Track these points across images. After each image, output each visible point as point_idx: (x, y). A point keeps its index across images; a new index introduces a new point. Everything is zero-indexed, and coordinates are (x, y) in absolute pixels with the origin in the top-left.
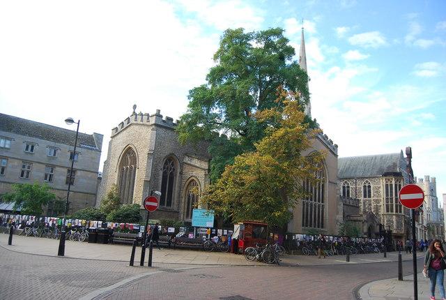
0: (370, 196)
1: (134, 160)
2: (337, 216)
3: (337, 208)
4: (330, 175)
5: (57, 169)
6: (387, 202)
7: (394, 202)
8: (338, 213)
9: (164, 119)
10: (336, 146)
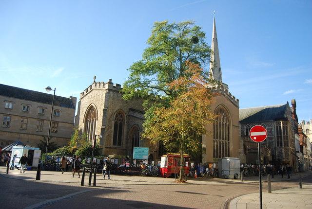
1: (95, 115)
3: (239, 144)
4: (234, 122)
5: (45, 122)
6: (278, 139)
9: (115, 85)
10: (238, 100)
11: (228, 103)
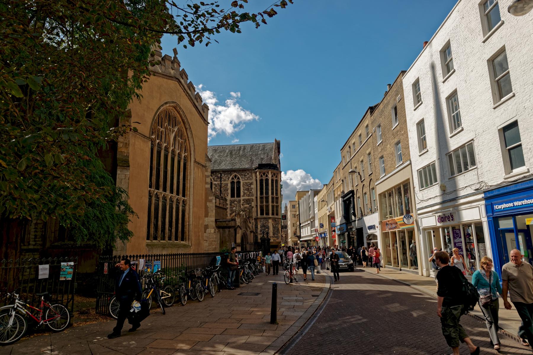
0: (239, 195)
2: (206, 219)
3: (206, 208)
4: (196, 155)
6: (262, 202)
7: (270, 204)
8: (206, 215)
11: (185, 104)
